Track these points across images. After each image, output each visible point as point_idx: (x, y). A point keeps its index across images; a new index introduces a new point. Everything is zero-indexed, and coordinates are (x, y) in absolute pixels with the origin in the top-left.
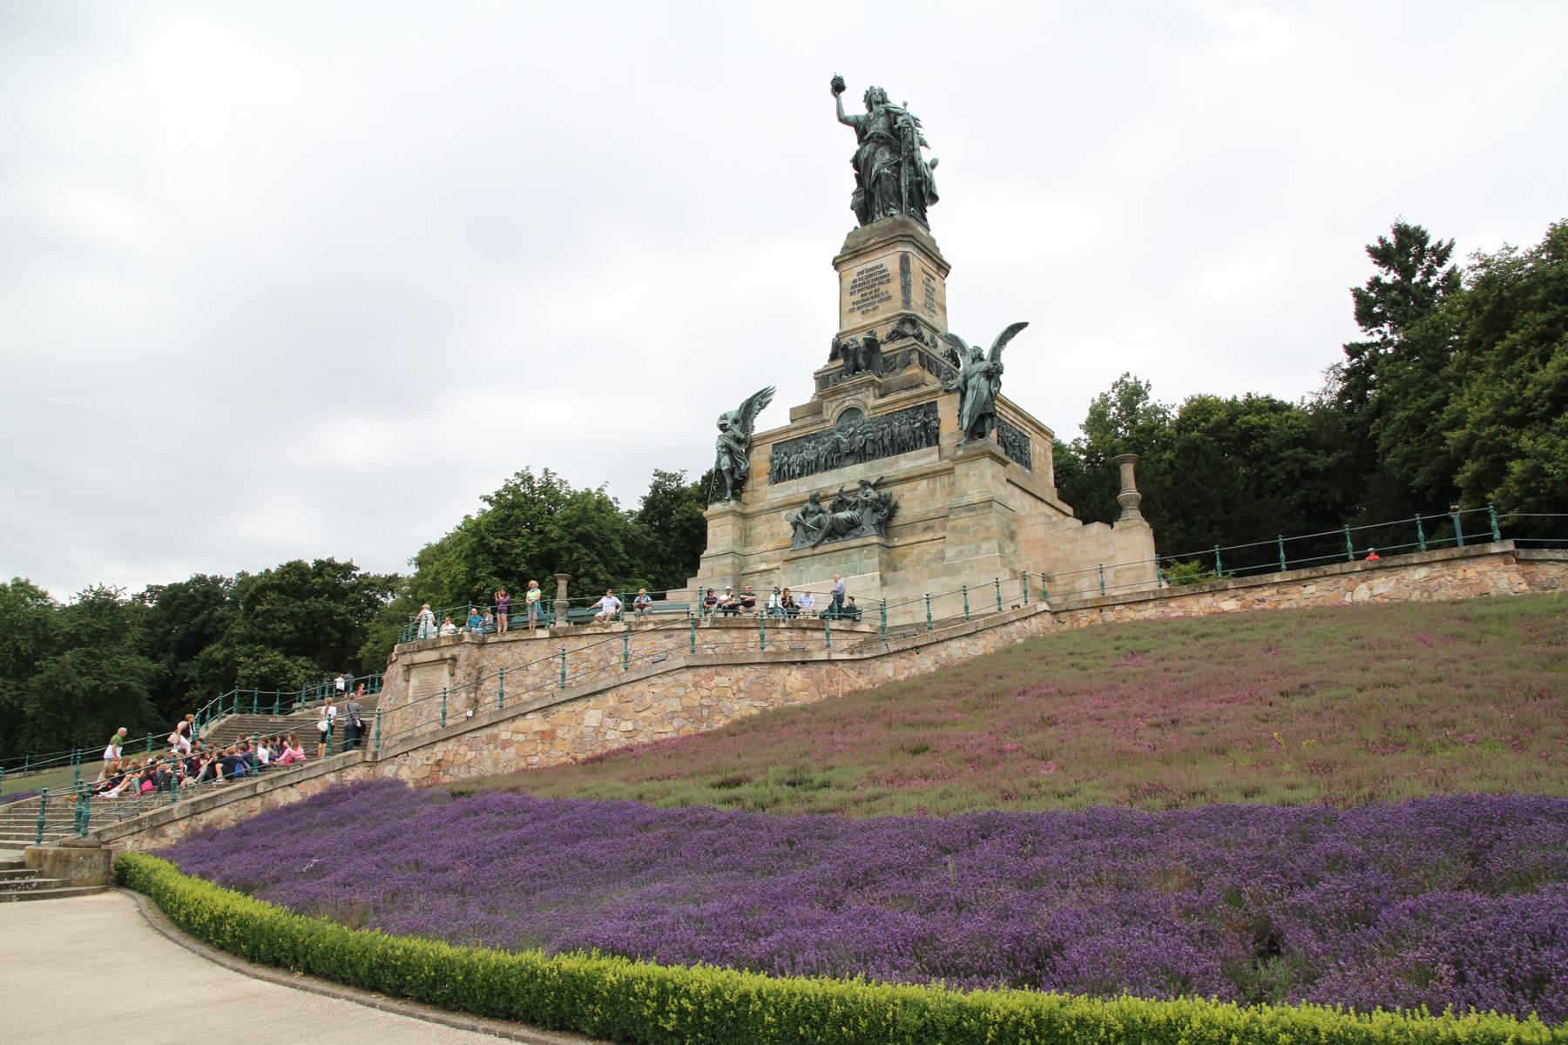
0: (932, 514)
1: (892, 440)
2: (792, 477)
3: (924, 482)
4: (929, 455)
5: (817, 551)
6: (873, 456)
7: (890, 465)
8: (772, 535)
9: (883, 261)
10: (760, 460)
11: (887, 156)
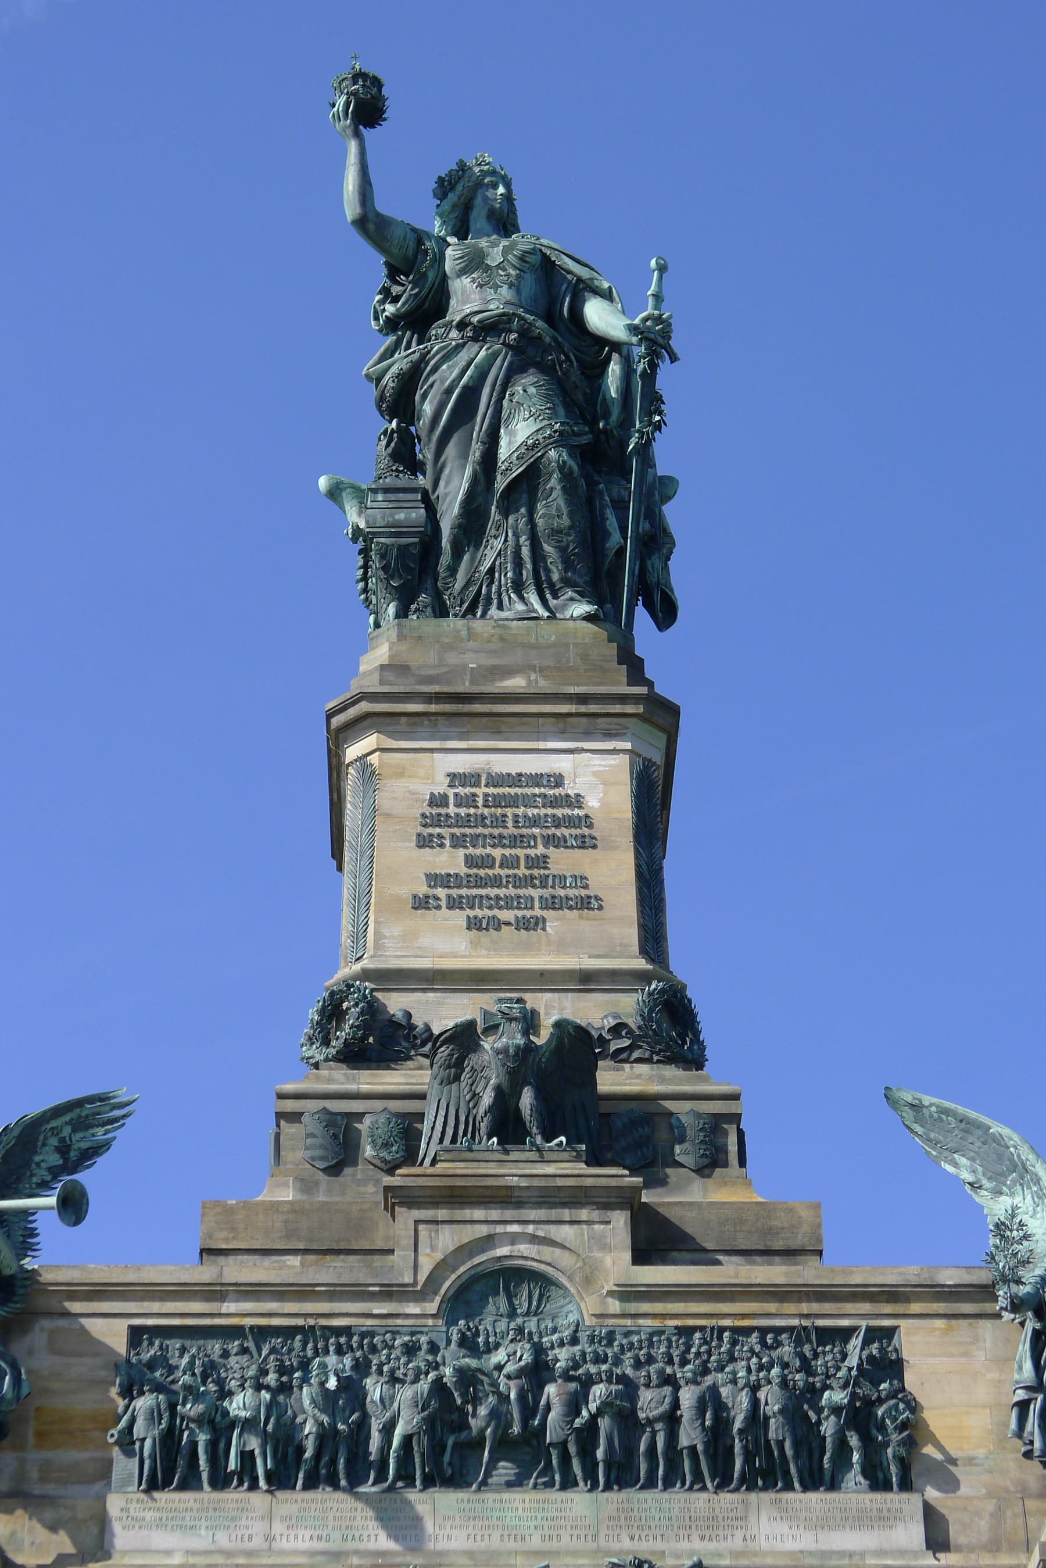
4: (884, 1520)
6: (621, 1474)
7: (712, 1525)
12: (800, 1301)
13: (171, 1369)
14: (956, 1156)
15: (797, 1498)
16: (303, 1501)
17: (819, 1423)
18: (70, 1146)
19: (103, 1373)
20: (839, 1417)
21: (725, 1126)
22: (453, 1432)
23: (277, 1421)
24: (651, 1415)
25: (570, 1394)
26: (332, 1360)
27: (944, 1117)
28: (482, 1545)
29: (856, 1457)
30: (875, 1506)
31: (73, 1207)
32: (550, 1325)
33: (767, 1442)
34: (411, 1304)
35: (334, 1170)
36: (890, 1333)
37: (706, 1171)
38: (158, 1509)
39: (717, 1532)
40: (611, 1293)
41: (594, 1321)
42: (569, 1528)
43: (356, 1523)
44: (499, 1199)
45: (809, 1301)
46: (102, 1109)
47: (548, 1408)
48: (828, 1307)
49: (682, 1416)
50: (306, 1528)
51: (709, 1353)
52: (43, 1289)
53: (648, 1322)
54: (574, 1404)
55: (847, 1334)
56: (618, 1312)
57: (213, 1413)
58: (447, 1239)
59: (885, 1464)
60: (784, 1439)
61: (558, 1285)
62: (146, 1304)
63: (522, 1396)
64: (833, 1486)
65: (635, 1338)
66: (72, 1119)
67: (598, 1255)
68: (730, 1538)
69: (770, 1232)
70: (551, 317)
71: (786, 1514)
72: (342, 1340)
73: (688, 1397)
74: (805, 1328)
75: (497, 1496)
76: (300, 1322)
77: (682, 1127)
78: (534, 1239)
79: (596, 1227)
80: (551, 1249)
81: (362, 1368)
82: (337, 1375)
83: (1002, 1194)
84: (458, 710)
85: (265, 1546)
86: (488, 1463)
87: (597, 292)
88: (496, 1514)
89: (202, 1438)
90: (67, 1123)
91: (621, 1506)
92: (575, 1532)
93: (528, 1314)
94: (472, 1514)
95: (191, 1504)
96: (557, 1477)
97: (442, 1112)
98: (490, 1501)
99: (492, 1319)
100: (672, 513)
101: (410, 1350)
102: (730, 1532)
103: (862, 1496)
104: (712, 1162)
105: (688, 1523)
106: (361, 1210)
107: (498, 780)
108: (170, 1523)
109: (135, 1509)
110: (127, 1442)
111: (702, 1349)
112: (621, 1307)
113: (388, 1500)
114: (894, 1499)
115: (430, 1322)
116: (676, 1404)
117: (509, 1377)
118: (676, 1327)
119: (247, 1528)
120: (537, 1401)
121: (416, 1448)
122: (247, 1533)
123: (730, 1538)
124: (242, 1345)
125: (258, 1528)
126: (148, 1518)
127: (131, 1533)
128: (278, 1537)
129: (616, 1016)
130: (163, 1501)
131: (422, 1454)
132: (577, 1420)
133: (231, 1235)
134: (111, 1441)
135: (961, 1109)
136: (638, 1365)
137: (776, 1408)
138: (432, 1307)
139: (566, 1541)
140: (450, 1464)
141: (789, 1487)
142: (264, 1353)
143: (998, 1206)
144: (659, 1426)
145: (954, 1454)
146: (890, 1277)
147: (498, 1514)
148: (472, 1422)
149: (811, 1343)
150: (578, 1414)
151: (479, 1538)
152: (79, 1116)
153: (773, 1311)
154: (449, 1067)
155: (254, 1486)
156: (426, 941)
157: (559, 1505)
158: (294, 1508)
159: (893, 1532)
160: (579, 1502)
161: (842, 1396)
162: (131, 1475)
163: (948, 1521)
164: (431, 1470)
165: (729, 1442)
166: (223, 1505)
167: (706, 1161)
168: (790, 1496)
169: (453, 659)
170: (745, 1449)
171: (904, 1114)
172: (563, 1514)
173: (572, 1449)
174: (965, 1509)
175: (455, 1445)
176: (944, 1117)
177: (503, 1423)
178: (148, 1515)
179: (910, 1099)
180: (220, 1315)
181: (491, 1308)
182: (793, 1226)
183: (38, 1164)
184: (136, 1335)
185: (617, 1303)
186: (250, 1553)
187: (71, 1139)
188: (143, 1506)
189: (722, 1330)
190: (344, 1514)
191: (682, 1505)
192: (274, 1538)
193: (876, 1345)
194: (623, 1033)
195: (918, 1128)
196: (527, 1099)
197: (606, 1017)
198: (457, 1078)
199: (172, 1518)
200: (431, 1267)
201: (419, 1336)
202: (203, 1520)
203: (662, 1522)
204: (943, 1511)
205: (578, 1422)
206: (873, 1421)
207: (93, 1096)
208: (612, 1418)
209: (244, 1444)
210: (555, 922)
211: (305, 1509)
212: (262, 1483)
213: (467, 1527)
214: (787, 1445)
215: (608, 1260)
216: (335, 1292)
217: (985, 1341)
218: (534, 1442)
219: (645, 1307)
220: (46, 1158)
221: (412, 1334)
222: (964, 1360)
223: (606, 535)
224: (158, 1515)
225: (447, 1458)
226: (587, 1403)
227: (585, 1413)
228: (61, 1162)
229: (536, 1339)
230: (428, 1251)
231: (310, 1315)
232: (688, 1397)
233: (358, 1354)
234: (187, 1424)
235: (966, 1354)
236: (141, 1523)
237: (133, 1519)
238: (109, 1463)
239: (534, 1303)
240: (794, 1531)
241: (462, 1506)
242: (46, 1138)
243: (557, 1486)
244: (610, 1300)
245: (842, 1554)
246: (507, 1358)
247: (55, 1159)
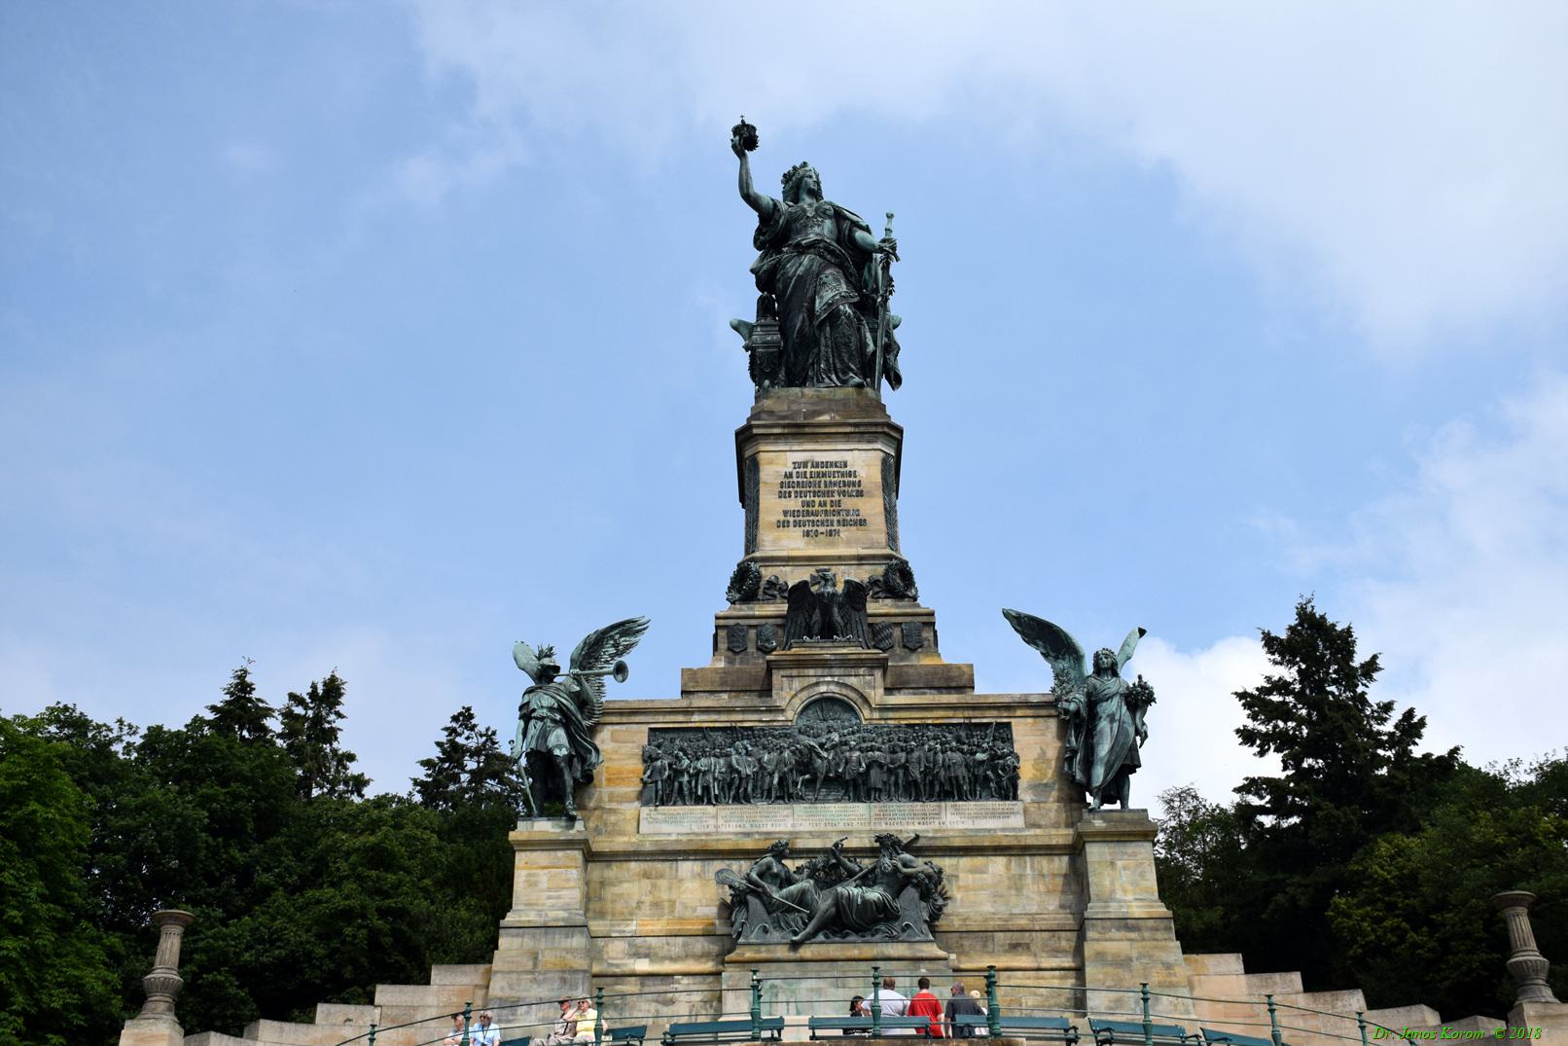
0: (1023, 922)
2: (699, 801)
4: (1006, 814)
5: (806, 952)
8: (656, 905)
9: (847, 457)
10: (619, 752)
11: (844, 288)
31: (621, 670)
48: (977, 713)
69: (950, 678)
70: (838, 241)
71: (957, 811)
84: (798, 431)
87: (861, 228)
100: (897, 334)
107: (816, 465)
125: (712, 822)
139: (856, 826)
155: (709, 803)
156: (784, 542)
160: (861, 808)
169: (794, 407)
210: (845, 533)
216: (744, 711)
219: (891, 715)
223: (866, 345)
247: (612, 651)
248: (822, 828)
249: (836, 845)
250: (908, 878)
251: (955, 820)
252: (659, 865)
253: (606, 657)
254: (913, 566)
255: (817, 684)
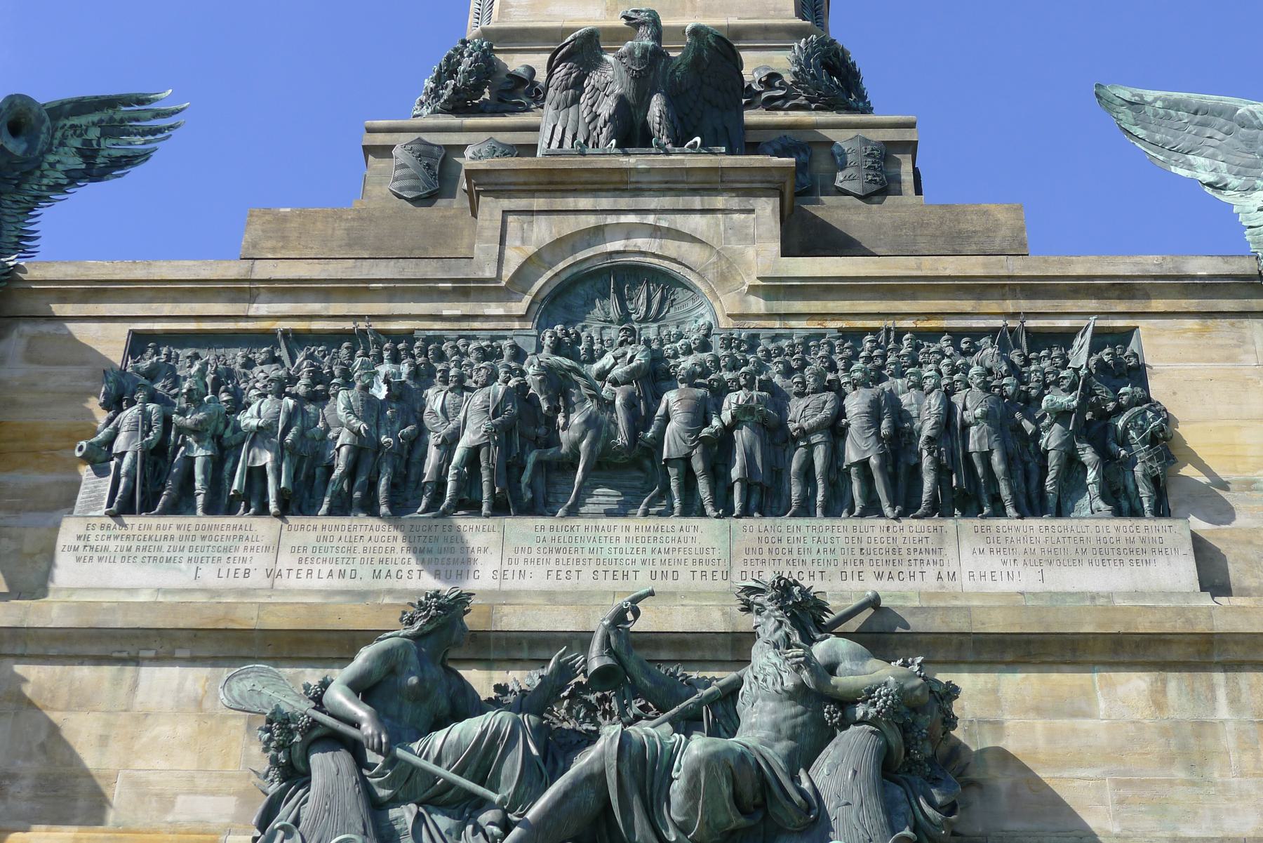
1: (898, 442)
3: (1134, 685)
4: (1138, 553)
6: (766, 498)
7: (893, 559)
12: (1003, 298)
13: (176, 381)
14: (1190, 157)
15: (1011, 525)
16: (324, 528)
17: (1037, 435)
18: (98, 150)
19: (89, 384)
20: (1065, 424)
21: (898, 156)
22: (538, 447)
23: (302, 434)
24: (806, 425)
25: (697, 399)
26: (385, 368)
27: (1173, 112)
28: (566, 585)
29: (1091, 475)
30: (1123, 535)
32: (674, 330)
33: (968, 456)
34: (493, 305)
35: (426, 199)
36: (1125, 336)
37: (876, 199)
38: (128, 537)
39: (900, 568)
40: (753, 290)
41: (731, 323)
42: (690, 562)
43: (393, 556)
44: (612, 186)
45: (1015, 297)
46: (142, 115)
47: (667, 418)
49: (848, 425)
50: (325, 561)
51: (884, 357)
52: (28, 289)
53: (803, 324)
54: (701, 414)
55: (1066, 338)
56: (763, 311)
57: (222, 426)
58: (543, 231)
59: (1132, 487)
60: (991, 451)
61: (686, 286)
62: (155, 305)
63: (631, 404)
64: (1060, 511)
65: (784, 343)
66: (101, 121)
67: (736, 246)
68: (918, 575)
71: (998, 546)
72: (401, 346)
73: (855, 404)
74: (1012, 330)
75: (591, 523)
76: (348, 325)
77: (843, 154)
78: (656, 232)
79: (736, 216)
80: (677, 243)
81: (423, 376)
82: (387, 381)
83: (1255, 189)
85: (266, 583)
86: (581, 484)
88: (588, 545)
89: (200, 454)
90: (94, 124)
91: (763, 535)
92: (698, 568)
93: (645, 319)
94: (555, 545)
95: (174, 531)
96: (677, 503)
97: (557, 136)
98: (582, 528)
99: (601, 323)
101: (488, 354)
102: (918, 569)
103: (1104, 523)
104: (882, 187)
105: (858, 556)
106: (444, 217)
108: (140, 554)
109: (95, 537)
110: (100, 457)
111: (876, 353)
112: (766, 306)
113: (440, 529)
114: (1148, 526)
115: (517, 325)
116: (840, 412)
117: (615, 383)
118: (840, 330)
119: (244, 560)
120: (651, 412)
121: (483, 464)
122: (242, 566)
123: (918, 575)
124: (271, 353)
125: (259, 562)
126: (112, 548)
127: (87, 565)
128: (285, 573)
129: (767, 68)
130: (136, 527)
131: (492, 471)
132: (705, 430)
133: (280, 244)
134: (78, 454)
135: (1195, 98)
136: (788, 372)
137: (978, 411)
138: (520, 307)
140: (530, 486)
141: (999, 512)
142: (298, 361)
143: (1252, 203)
144: (816, 438)
145: (1223, 476)
146: (1122, 266)
147: (592, 545)
148: (563, 436)
149: (1020, 347)
150: (707, 423)
151: (563, 575)
152: (111, 119)
153: (969, 310)
154: (566, 88)
155: (263, 510)
157: (677, 534)
158: (312, 536)
159: (1152, 567)
161: (1070, 397)
162: (101, 497)
163: (1223, 558)
164: (502, 491)
165: (914, 460)
166: (214, 533)
167: (875, 187)
168: (1002, 522)
170: (937, 463)
171: (1120, 116)
172: (683, 545)
173: (698, 465)
174: (1250, 542)
175: (539, 464)
176: (1173, 112)
177: (604, 435)
178: (112, 544)
179: (1128, 96)
180: (247, 318)
181: (597, 312)
182: (988, 229)
183: (52, 165)
184: (138, 343)
185: (762, 301)
186: (243, 592)
187: (99, 144)
188: (109, 533)
189: (900, 333)
190: (378, 545)
191: (850, 534)
192: (280, 574)
193: (1107, 351)
194: (777, 84)
195: (1139, 131)
196: (656, 106)
197: (756, 69)
198: (576, 100)
199: (144, 549)
200: (521, 261)
201: (501, 342)
202: (186, 550)
203: (822, 556)
204: (1218, 545)
205: (705, 432)
206: (1111, 435)
207: (130, 96)
208: (752, 429)
209: (254, 459)
211: (325, 538)
212: (273, 507)
213: (548, 562)
214: (996, 458)
215: (750, 252)
217: (1254, 343)
218: (647, 463)
220: (64, 159)
221: (493, 339)
222: (1228, 365)
224: (126, 544)
225: (525, 478)
226: (719, 413)
227: (715, 423)
228: (84, 166)
229: (654, 346)
230: (518, 243)
231: (361, 317)
232: (855, 404)
233: (420, 360)
234: (184, 438)
235: (1228, 359)
236: (100, 554)
237: (92, 548)
238: (76, 485)
239: (655, 306)
240: (1010, 567)
241: (542, 534)
242: (64, 137)
243: (676, 511)
244: (752, 298)
245: (1081, 595)
246: (616, 361)
247: (77, 163)
248: (585, 581)
249: (619, 618)
250: (845, 702)
251: (982, 569)
252: (85, 673)
253: (58, 175)
254: (857, 57)
255: (597, 233)
